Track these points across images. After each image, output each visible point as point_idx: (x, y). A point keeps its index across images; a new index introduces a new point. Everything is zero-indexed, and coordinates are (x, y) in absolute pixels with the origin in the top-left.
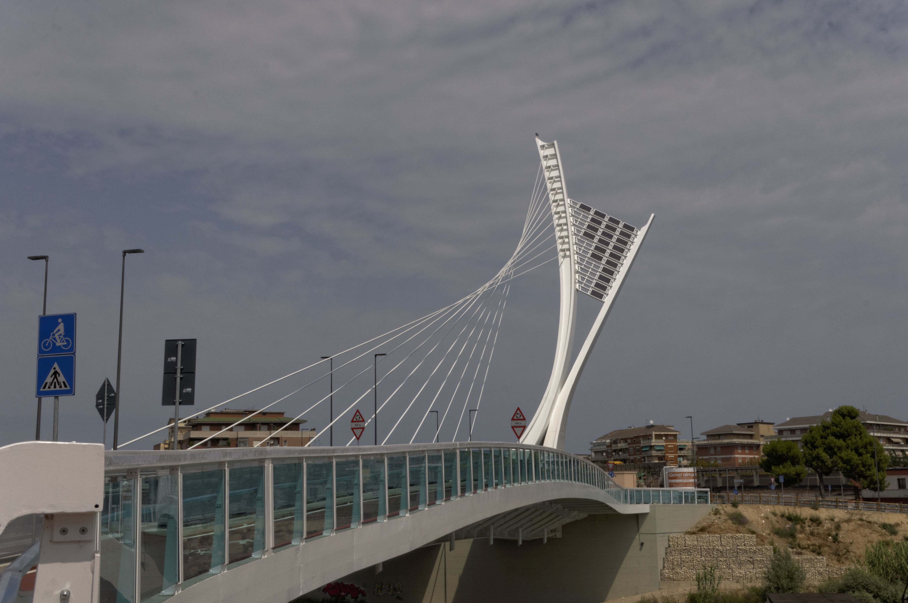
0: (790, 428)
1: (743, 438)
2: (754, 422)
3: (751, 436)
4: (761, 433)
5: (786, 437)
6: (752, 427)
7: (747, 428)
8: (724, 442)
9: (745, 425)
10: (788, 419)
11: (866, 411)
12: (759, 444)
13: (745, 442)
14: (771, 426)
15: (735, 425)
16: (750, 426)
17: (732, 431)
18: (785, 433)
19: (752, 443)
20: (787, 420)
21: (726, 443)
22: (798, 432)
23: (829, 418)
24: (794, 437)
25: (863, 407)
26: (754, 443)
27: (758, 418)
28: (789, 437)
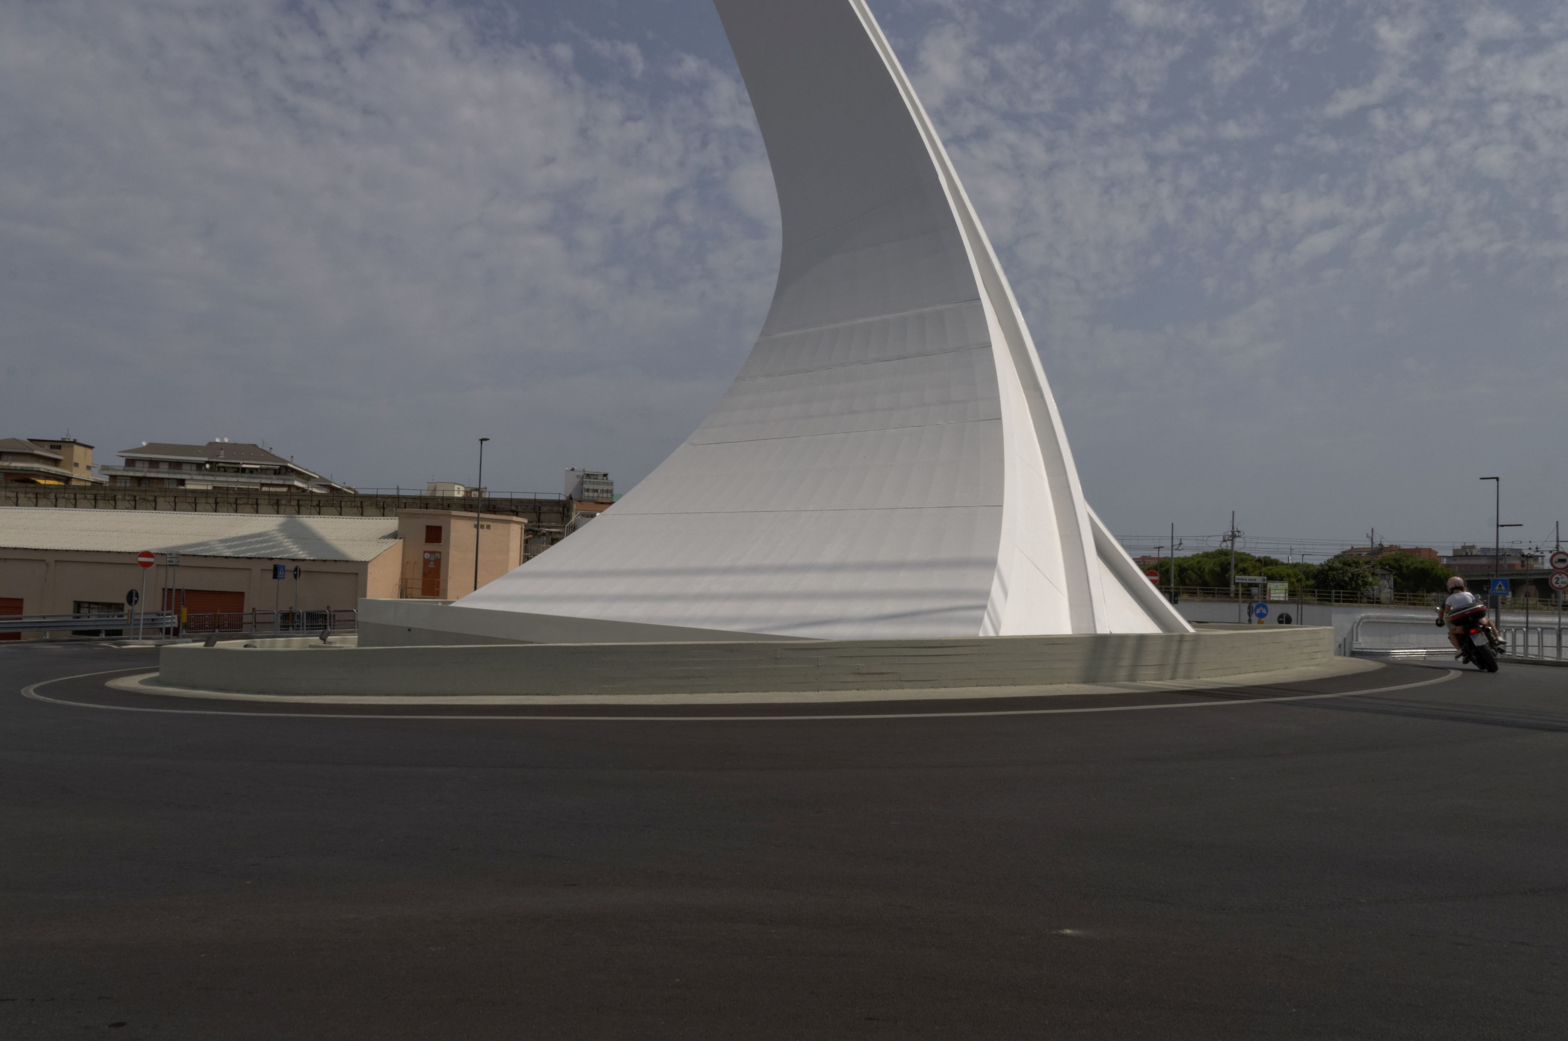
0: (151, 458)
1: (44, 463)
2: (60, 439)
3: (56, 462)
4: (75, 460)
5: (142, 471)
6: (59, 447)
7: (49, 448)
8: (16, 467)
9: (46, 443)
10: (144, 444)
11: (271, 448)
12: (70, 476)
13: (52, 471)
14: (89, 451)
15: (26, 440)
16: (56, 445)
17: (33, 450)
18: (139, 465)
19: (62, 474)
20: (142, 445)
21: (18, 469)
22: (164, 467)
23: (222, 452)
24: (157, 472)
25: (263, 442)
26: (65, 473)
27: (67, 435)
28: (149, 472)
